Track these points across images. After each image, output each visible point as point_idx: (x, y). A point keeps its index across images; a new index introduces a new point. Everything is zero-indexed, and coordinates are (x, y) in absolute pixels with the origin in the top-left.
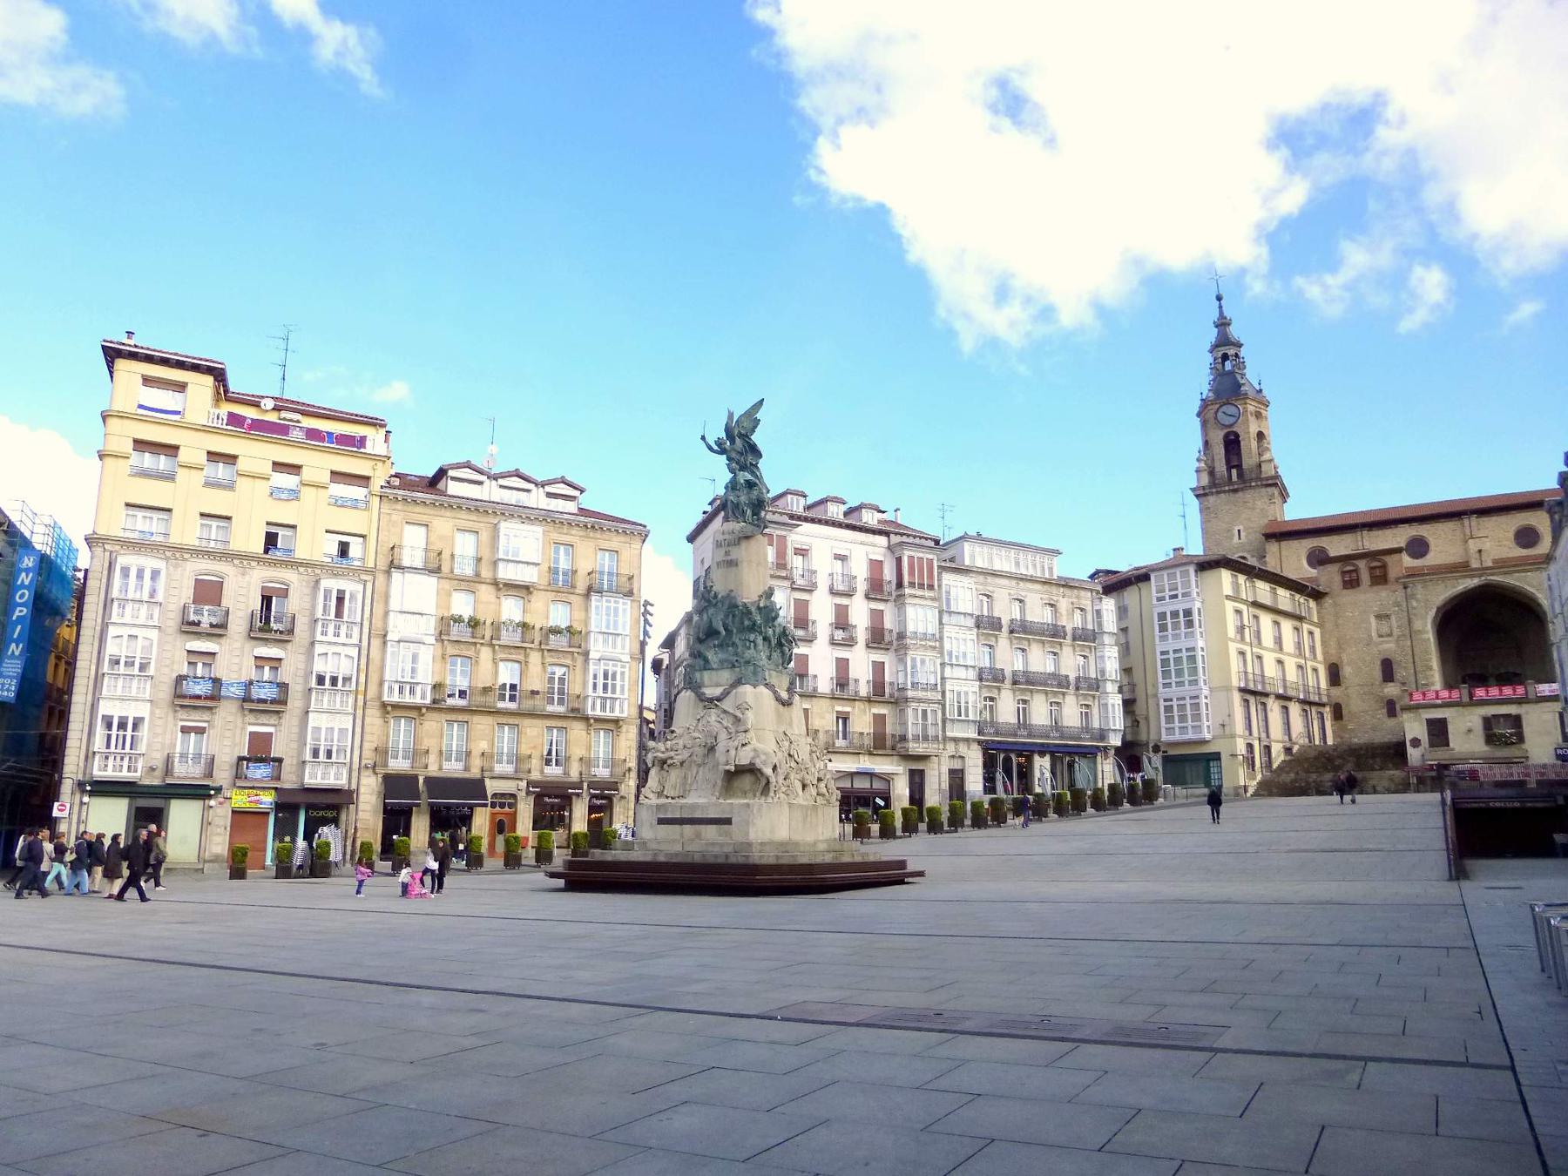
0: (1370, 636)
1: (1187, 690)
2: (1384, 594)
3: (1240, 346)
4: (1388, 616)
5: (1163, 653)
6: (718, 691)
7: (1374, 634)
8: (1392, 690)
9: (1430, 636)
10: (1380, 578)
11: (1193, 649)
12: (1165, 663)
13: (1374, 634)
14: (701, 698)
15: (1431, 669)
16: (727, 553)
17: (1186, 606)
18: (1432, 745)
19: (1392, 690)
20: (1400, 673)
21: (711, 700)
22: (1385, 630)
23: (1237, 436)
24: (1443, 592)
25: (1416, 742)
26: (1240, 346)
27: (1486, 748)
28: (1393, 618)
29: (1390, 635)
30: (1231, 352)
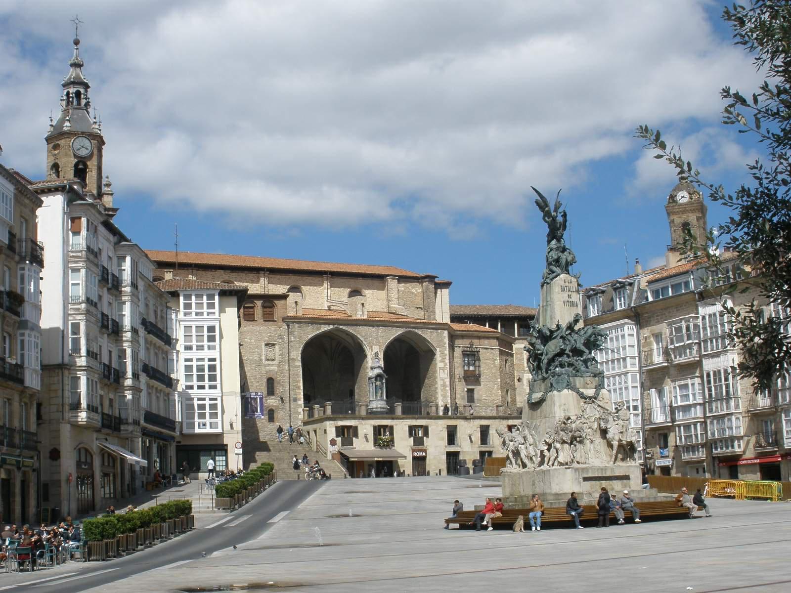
0: (261, 359)
1: (216, 393)
2: (273, 329)
3: (89, 87)
4: (274, 345)
5: (186, 360)
6: (590, 392)
7: (263, 358)
8: (272, 402)
9: (300, 364)
10: (268, 317)
11: (214, 360)
12: (188, 368)
13: (263, 358)
14: (582, 396)
15: (299, 388)
16: (569, 296)
17: (211, 324)
18: (343, 444)
19: (272, 402)
20: (279, 389)
21: (590, 398)
22: (271, 356)
23: (86, 166)
24: (311, 332)
25: (333, 442)
26: (86, 86)
27: (373, 448)
28: (277, 347)
29: (273, 360)
30: (82, 91)
